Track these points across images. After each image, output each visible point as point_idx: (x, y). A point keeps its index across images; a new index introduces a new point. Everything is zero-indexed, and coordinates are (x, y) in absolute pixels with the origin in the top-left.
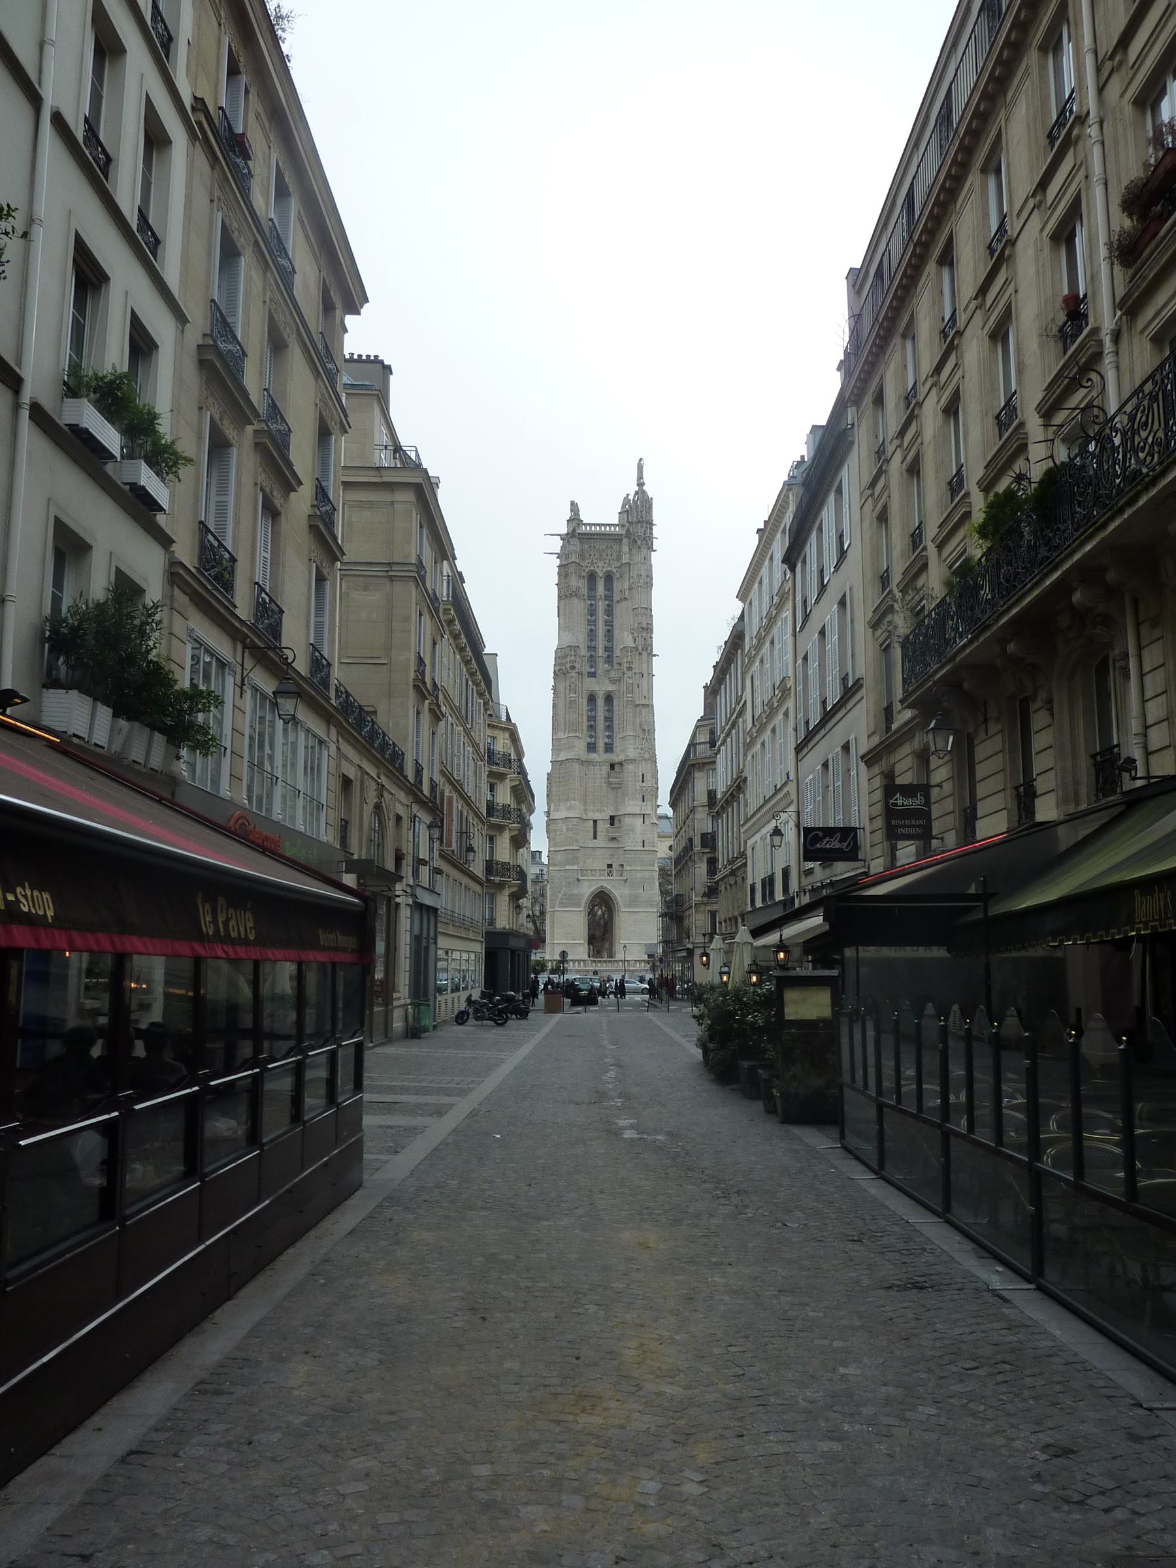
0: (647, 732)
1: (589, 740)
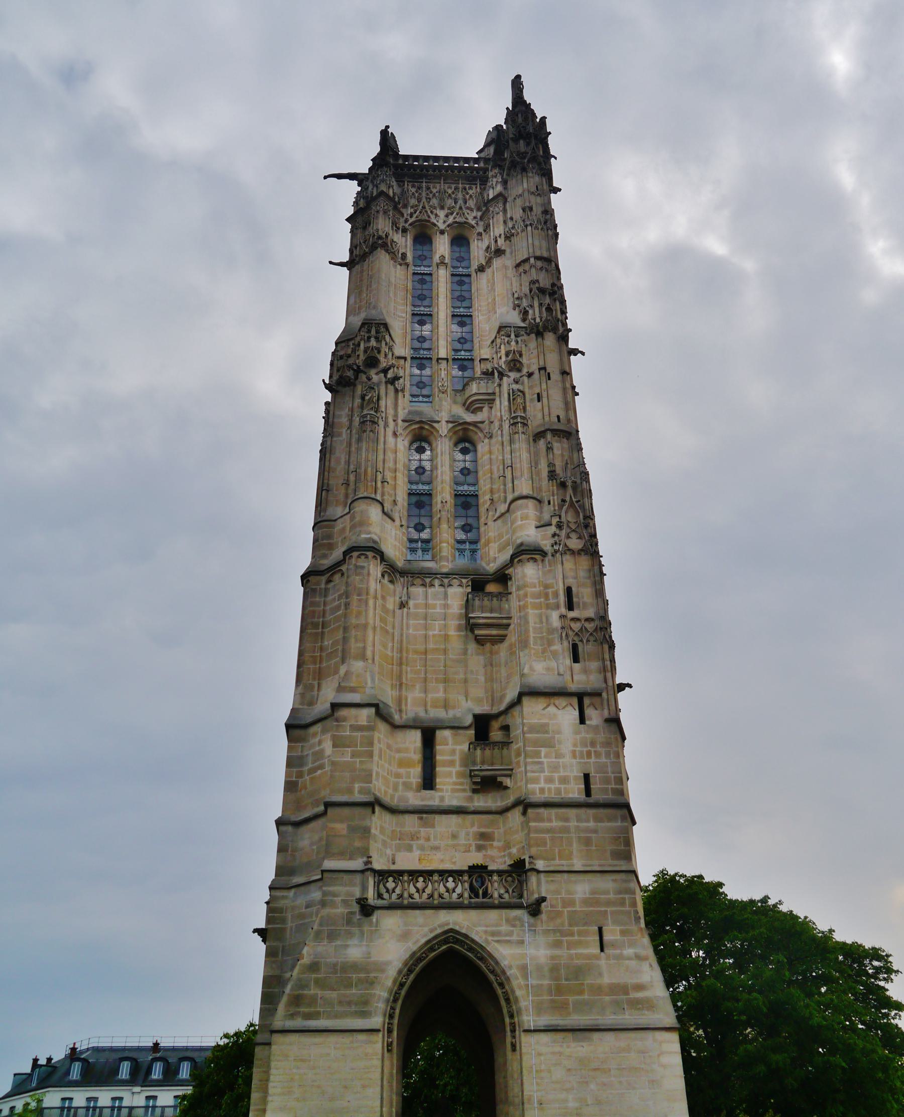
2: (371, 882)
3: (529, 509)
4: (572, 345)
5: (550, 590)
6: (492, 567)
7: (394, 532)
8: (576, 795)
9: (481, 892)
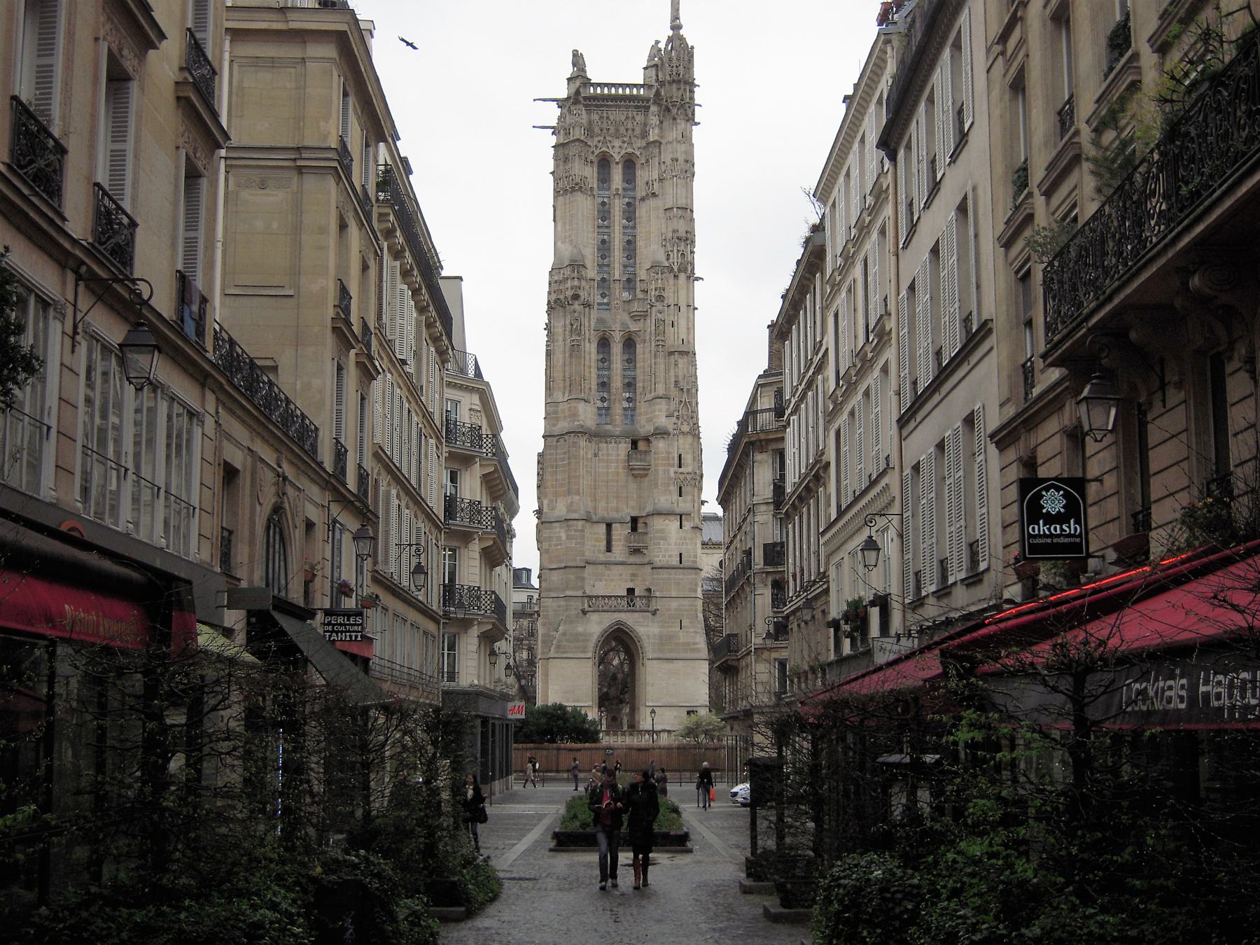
0: (685, 394)
1: (599, 404)
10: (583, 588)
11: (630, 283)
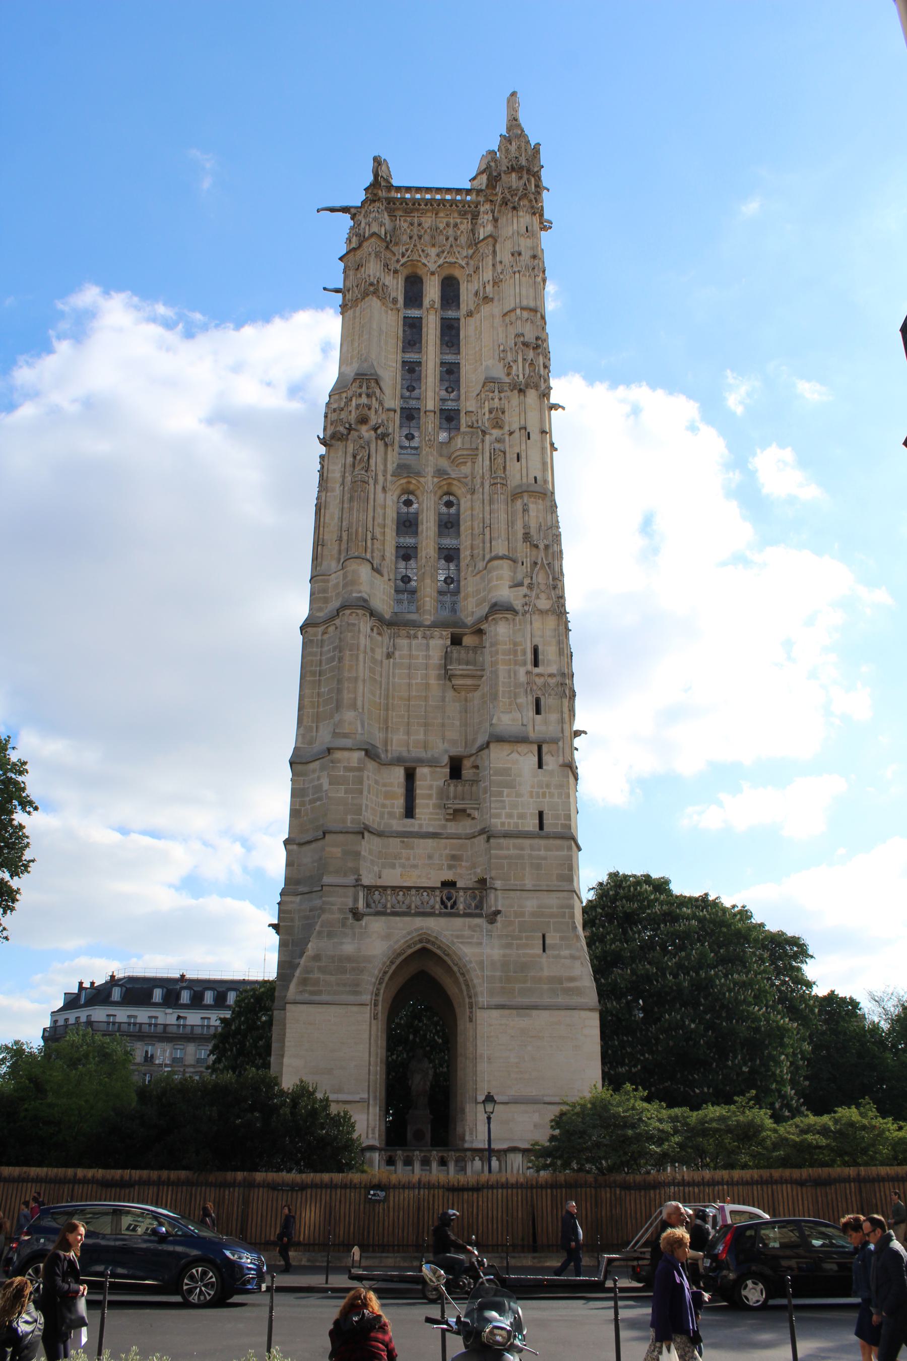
2: (361, 894)
3: (504, 570)
4: (553, 400)
5: (519, 648)
6: (469, 620)
7: (382, 587)
8: (531, 829)
9: (449, 905)
10: (356, 871)
11: (450, 418)
